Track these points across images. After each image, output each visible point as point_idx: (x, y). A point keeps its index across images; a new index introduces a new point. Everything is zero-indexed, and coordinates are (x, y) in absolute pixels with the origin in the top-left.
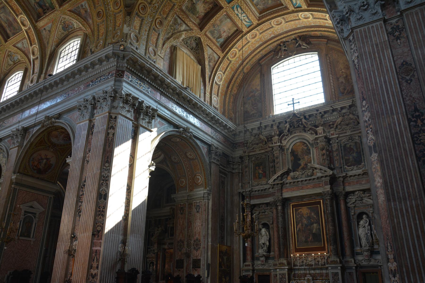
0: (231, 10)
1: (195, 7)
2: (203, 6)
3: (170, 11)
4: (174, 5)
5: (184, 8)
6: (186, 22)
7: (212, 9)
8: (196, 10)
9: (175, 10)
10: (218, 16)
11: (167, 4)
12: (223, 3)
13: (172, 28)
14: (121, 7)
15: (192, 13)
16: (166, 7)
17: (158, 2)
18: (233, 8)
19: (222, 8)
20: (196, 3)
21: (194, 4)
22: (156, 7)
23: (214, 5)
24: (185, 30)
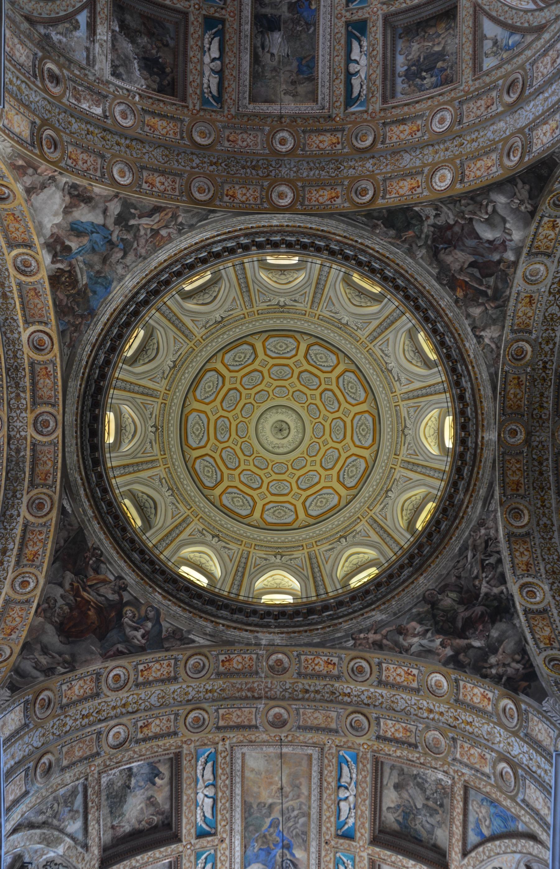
0: (192, 858)
1: (125, 795)
2: (142, 808)
3: (81, 760)
4: (98, 754)
5: (104, 780)
6: (90, 816)
7: (154, 829)
8: (122, 807)
9: (90, 766)
10: (158, 855)
11: (88, 738)
12: (188, 827)
13: (56, 805)
14: (5, 664)
15: (111, 807)
16: (81, 745)
17: (76, 720)
18: (198, 857)
19: (176, 838)
20: (134, 788)
21: (129, 787)
22: (64, 725)
23: (163, 822)
24: (72, 837)
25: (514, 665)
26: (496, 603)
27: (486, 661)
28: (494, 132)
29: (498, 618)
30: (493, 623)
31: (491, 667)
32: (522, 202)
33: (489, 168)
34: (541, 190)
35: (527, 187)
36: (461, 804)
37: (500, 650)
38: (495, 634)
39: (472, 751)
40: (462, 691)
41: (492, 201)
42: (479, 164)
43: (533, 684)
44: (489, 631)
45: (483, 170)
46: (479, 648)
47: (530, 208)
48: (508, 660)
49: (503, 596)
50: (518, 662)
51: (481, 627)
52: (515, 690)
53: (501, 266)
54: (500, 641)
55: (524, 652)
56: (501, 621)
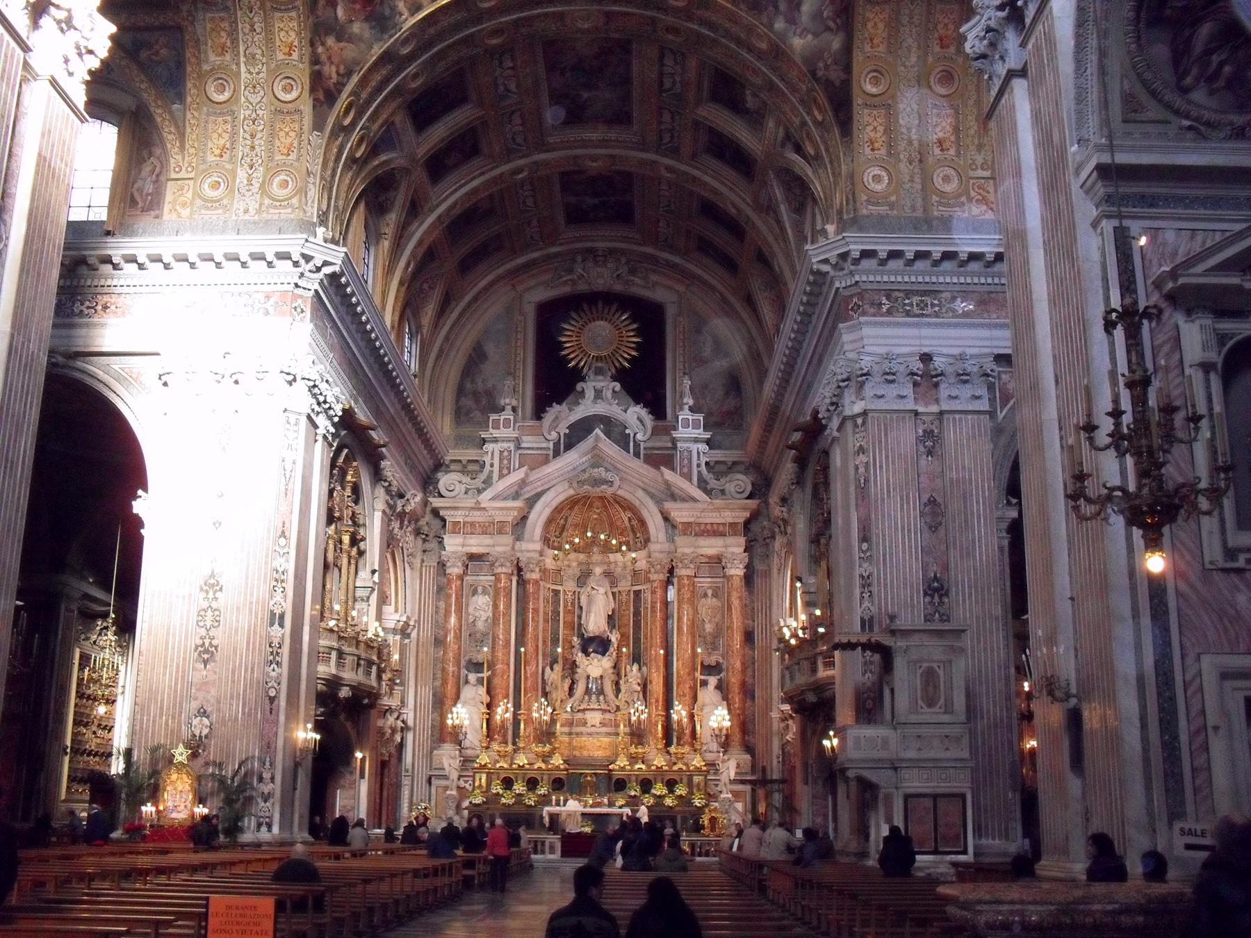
25: (334, 69)
26: (387, 12)
27: (327, 34)
28: (909, 49)
29: (374, 23)
30: (367, 20)
31: (323, 44)
32: (827, 67)
33: (871, 40)
34: (831, 100)
35: (837, 83)
36: (157, 23)
37: (342, 44)
38: (356, 28)
39: (223, 34)
40: (286, 15)
41: (838, 29)
42: (881, 25)
43: (325, 107)
44: (357, 19)
45: (872, 31)
46: (336, 17)
47: (820, 74)
48: (335, 60)
49: (397, 17)
50: (338, 73)
51: (358, 6)
52: (313, 90)
53: (771, 8)
54: (351, 39)
55: (349, 74)
56: (371, 28)
